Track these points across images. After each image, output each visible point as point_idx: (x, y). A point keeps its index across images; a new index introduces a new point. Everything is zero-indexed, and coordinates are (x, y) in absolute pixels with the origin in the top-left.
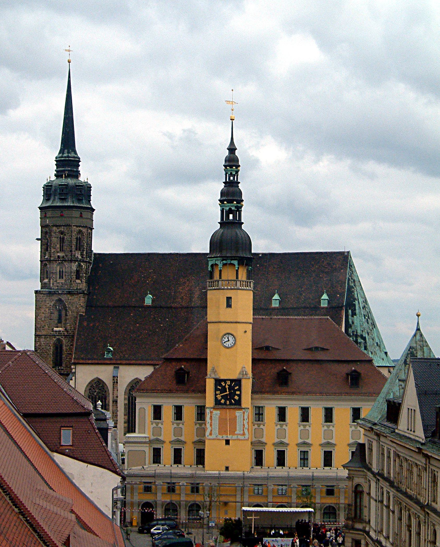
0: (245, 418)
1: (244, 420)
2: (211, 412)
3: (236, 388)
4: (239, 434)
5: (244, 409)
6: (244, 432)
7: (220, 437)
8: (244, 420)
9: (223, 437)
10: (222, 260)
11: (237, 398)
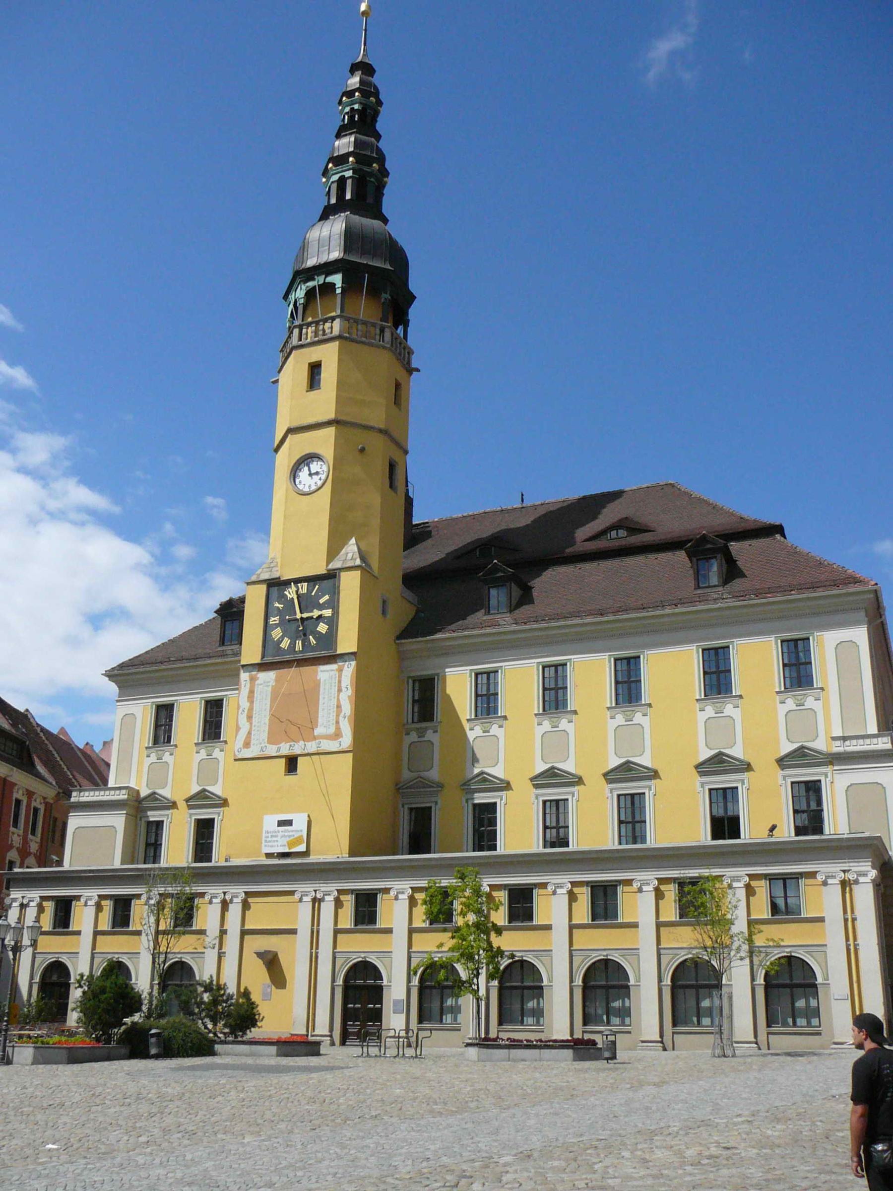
0: (343, 685)
1: (340, 690)
2: (253, 679)
3: (321, 601)
5: (342, 656)
6: (338, 728)
7: (272, 750)
8: (340, 690)
9: (279, 750)
10: (305, 282)
11: (322, 628)
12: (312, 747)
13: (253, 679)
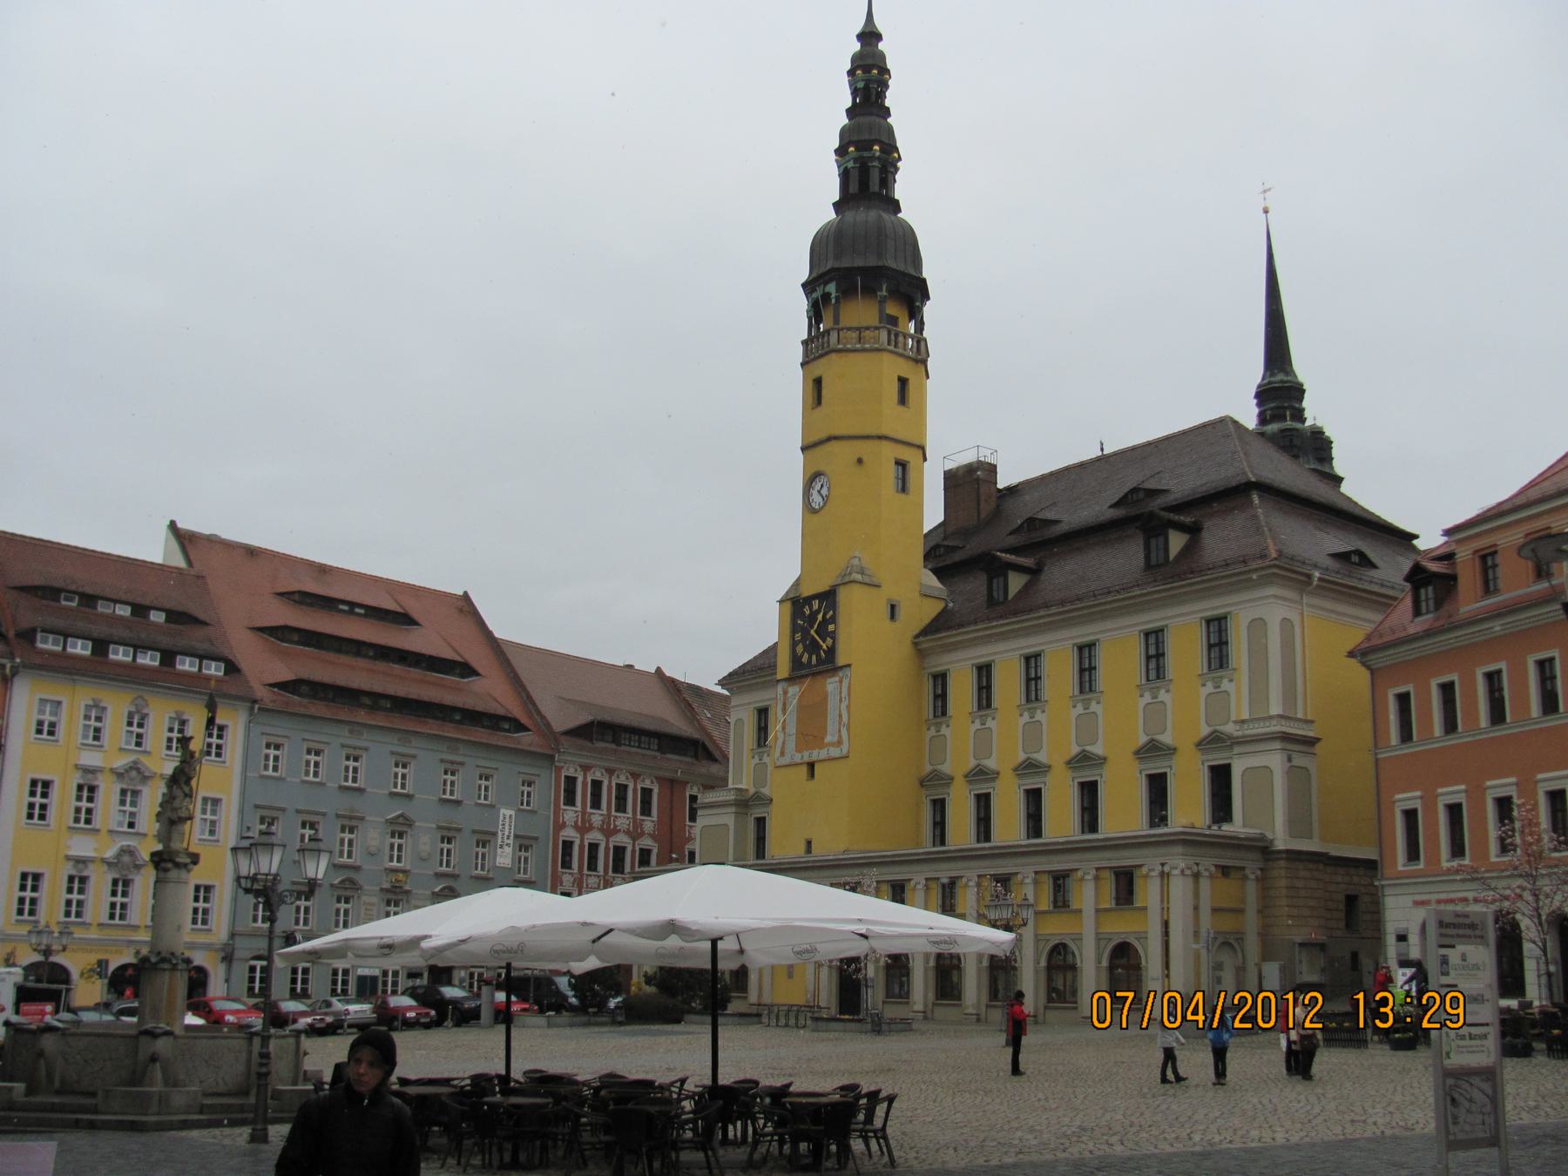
2: (785, 693)
4: (832, 744)
5: (841, 668)
7: (798, 758)
12: (823, 754)
13: (785, 693)
